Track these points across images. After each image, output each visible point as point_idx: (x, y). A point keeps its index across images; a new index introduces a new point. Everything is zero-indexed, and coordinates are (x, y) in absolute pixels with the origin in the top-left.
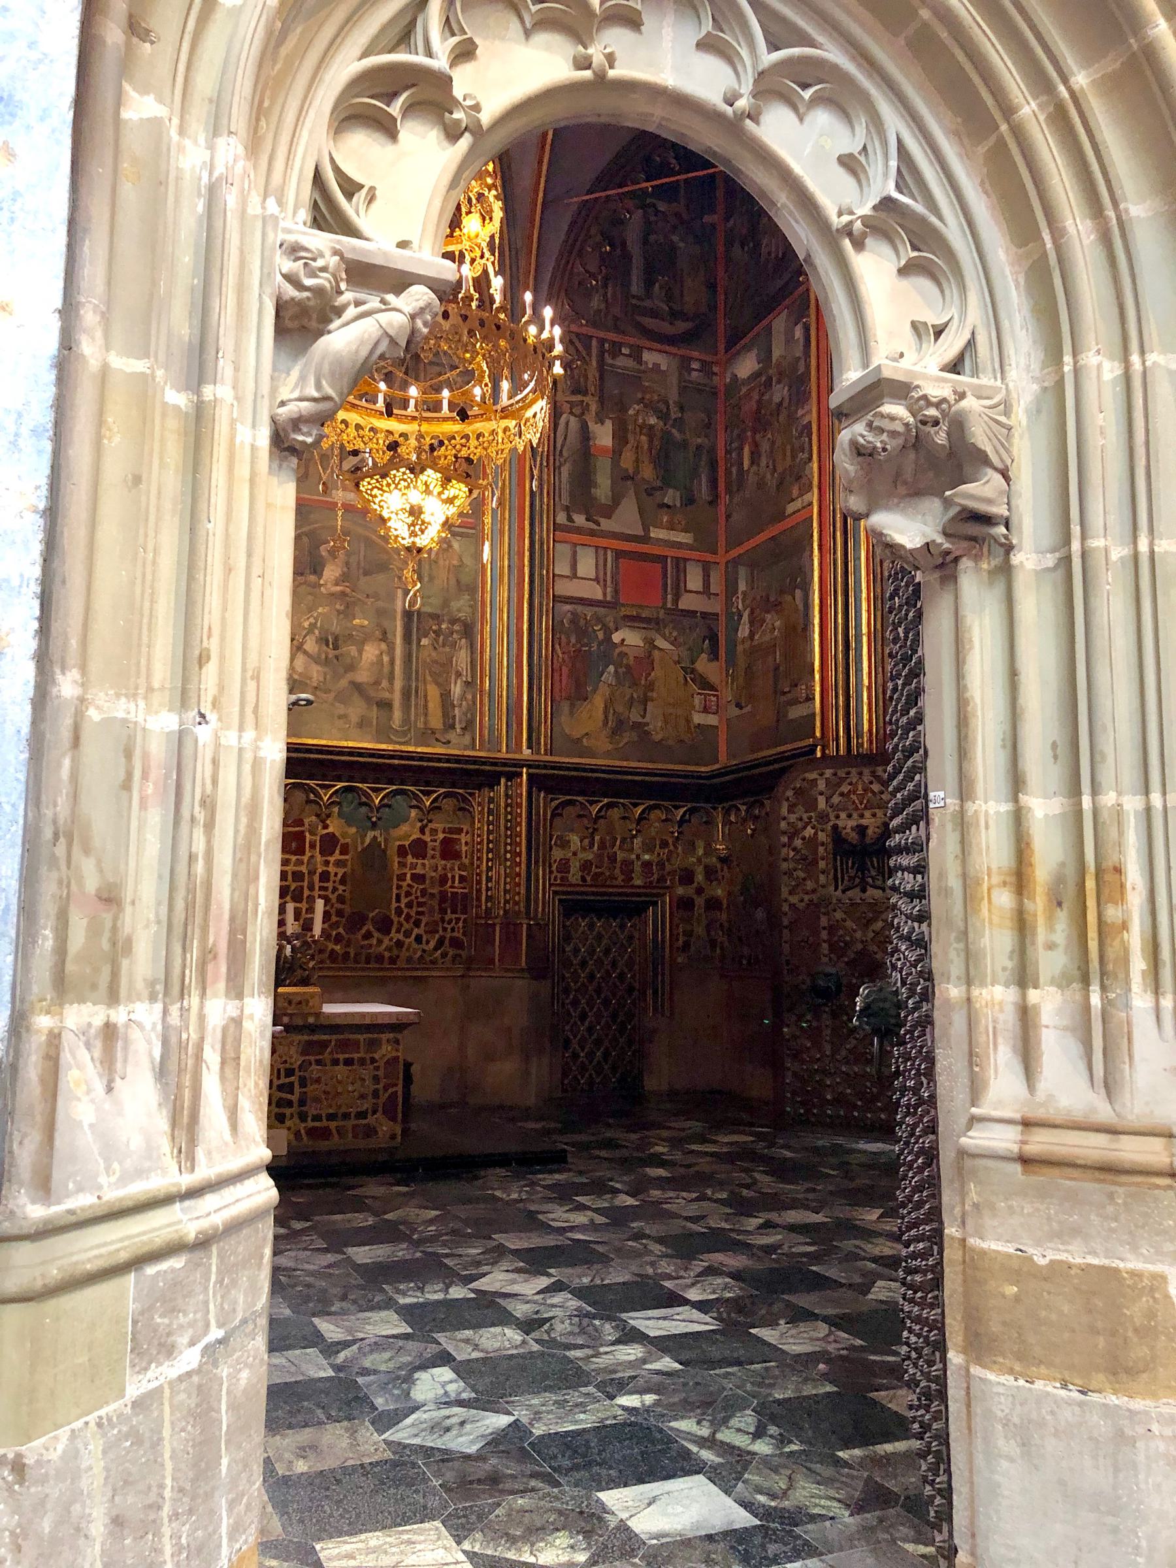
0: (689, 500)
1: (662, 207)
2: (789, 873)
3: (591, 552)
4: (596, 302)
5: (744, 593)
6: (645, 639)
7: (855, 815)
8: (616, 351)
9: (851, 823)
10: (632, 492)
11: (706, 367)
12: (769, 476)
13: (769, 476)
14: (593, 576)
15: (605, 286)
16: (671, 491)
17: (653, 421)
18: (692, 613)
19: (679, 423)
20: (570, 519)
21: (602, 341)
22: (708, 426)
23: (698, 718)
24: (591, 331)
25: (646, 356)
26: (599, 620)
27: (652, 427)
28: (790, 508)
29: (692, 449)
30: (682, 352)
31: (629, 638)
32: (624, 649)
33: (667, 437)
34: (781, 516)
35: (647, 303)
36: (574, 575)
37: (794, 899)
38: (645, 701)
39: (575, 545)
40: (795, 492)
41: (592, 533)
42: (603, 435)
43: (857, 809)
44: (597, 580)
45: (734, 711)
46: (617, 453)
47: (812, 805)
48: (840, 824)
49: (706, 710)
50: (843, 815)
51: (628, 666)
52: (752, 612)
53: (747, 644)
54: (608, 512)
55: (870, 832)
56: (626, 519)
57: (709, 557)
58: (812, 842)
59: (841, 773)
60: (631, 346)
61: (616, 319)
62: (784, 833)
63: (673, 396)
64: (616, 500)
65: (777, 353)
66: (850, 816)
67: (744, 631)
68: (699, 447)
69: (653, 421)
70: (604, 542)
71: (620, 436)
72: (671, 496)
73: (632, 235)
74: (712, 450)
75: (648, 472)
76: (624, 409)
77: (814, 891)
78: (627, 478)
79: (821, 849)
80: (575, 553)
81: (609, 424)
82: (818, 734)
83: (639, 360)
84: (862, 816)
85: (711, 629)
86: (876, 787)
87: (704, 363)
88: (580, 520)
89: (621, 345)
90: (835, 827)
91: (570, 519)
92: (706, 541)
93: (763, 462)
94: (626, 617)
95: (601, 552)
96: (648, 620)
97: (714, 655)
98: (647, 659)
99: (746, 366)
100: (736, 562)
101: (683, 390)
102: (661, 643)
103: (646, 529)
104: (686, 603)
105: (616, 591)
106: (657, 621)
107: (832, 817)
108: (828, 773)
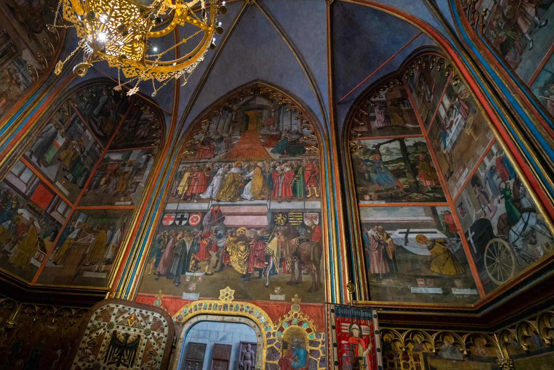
0: (74, 182)
1: (113, 101)
2: (83, 349)
3: (31, 174)
4: (82, 104)
5: (80, 223)
6: (31, 219)
7: (126, 328)
8: (80, 122)
9: (123, 332)
10: (58, 165)
11: (100, 149)
12: (111, 190)
13: (111, 190)
14: (26, 181)
15: (88, 103)
16: (70, 175)
17: (78, 150)
18: (53, 219)
19: (85, 157)
20: (31, 156)
21: (77, 116)
22: (92, 165)
23: (33, 261)
24: (76, 109)
25: (87, 131)
26: (17, 199)
27: (77, 151)
28: (117, 203)
29: (84, 167)
30: (97, 139)
31: (25, 214)
32: (20, 217)
33: (79, 159)
34: (113, 204)
35: (96, 119)
36: (19, 177)
37: (80, 364)
38: (15, 243)
39: (27, 167)
40: (122, 199)
41: (36, 167)
42: (60, 141)
43: (128, 326)
44: (27, 185)
45: (50, 264)
46: (61, 149)
47: (107, 319)
48: (118, 330)
49: (38, 259)
50: (121, 327)
51: (17, 225)
52: (81, 230)
53: (72, 241)
54: (46, 165)
55: (131, 337)
56: (51, 172)
57: (70, 203)
58: (102, 336)
59: (127, 308)
60: (85, 125)
61: (85, 114)
62: (89, 329)
63: (88, 149)
64: (52, 163)
65: (131, 158)
66: (124, 328)
67: (73, 235)
68: (86, 169)
69: (78, 150)
70: (38, 174)
71: (66, 146)
72: (69, 176)
73: (102, 100)
74: (89, 173)
75: (67, 164)
76: (72, 138)
77: (93, 361)
78: (59, 159)
79: (104, 341)
80: (24, 169)
81: (64, 140)
82: (110, 287)
83: (84, 130)
84: (129, 329)
85: (57, 228)
86: (140, 318)
87: (100, 147)
88: (34, 159)
89: (82, 122)
90: (115, 332)
91: (31, 156)
92: (72, 198)
93: (111, 185)
94: (29, 205)
95: (35, 176)
96: (36, 212)
97: (53, 240)
98: (27, 227)
99: (116, 157)
100: (80, 211)
101: (92, 149)
102: (36, 224)
103: (56, 180)
104: (54, 214)
105: (31, 194)
106: (40, 214)
107: (115, 326)
108: (121, 306)
